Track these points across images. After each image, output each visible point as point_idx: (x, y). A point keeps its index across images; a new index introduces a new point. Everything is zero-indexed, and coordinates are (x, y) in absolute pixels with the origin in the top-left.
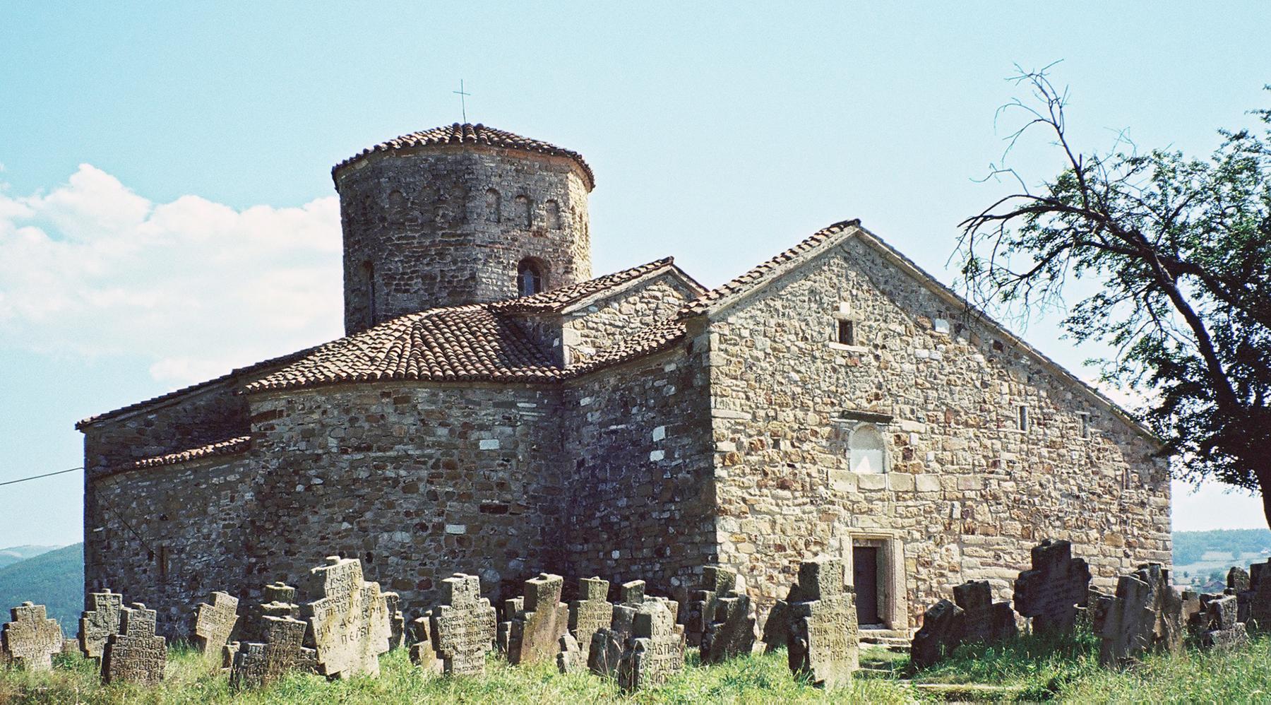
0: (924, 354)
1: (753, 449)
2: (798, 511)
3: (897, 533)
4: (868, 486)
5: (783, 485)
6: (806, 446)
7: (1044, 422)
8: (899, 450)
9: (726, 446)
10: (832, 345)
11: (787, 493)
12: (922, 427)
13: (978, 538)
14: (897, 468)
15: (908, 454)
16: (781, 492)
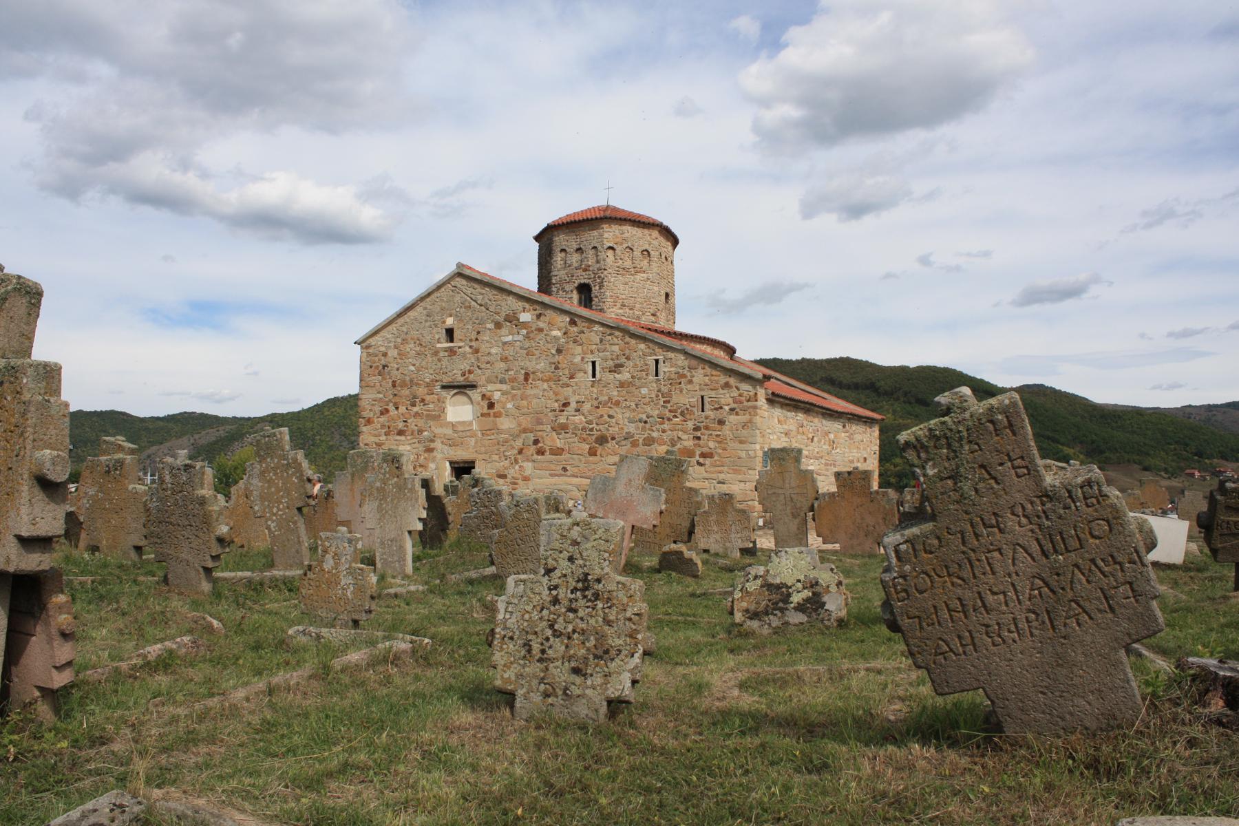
0: (510, 338)
1: (382, 413)
2: (408, 448)
3: (483, 456)
4: (461, 428)
5: (401, 433)
6: (415, 409)
7: (617, 368)
8: (485, 404)
9: (365, 414)
10: (439, 345)
11: (403, 438)
12: (504, 387)
13: (548, 457)
14: (482, 415)
15: (491, 406)
16: (398, 438)
